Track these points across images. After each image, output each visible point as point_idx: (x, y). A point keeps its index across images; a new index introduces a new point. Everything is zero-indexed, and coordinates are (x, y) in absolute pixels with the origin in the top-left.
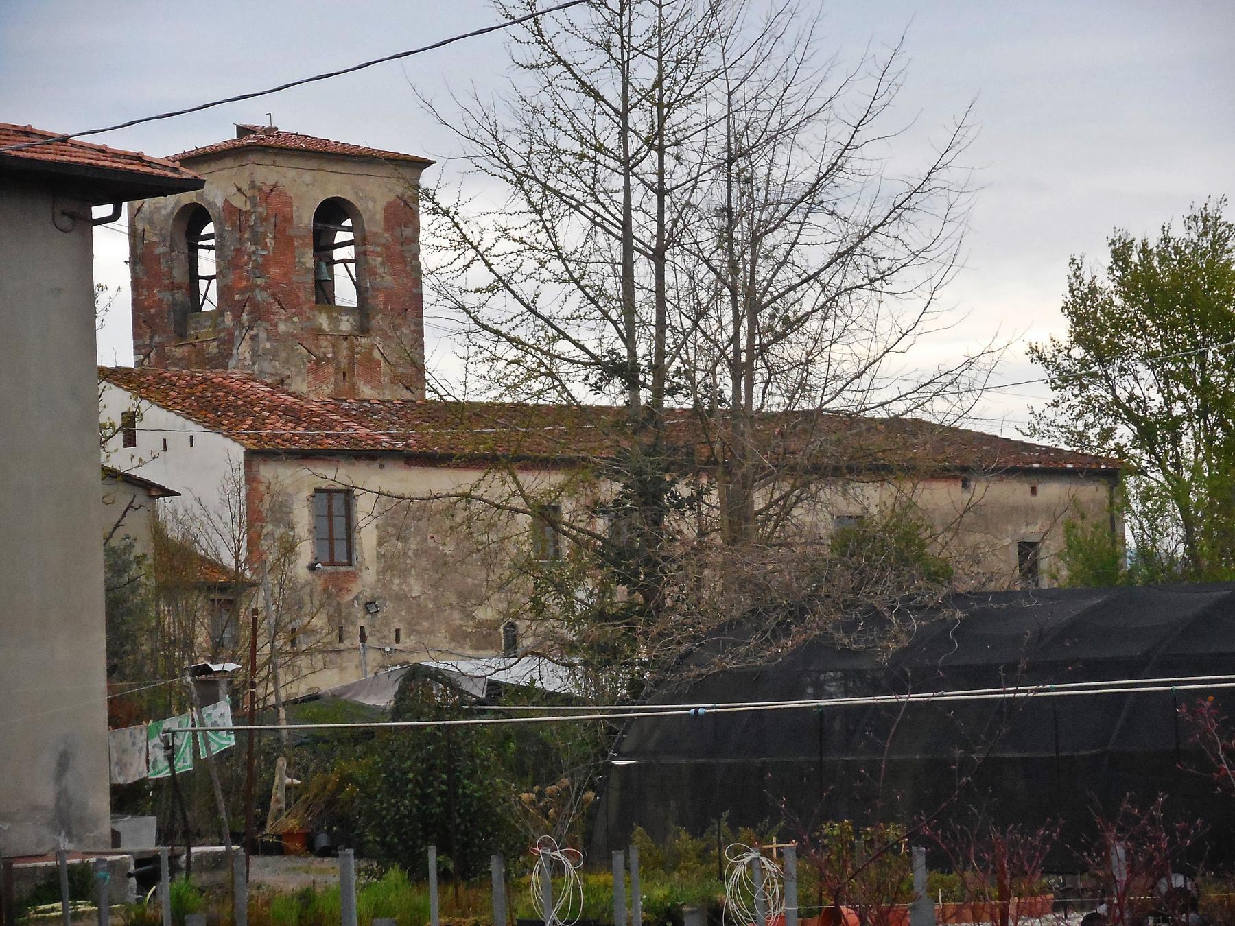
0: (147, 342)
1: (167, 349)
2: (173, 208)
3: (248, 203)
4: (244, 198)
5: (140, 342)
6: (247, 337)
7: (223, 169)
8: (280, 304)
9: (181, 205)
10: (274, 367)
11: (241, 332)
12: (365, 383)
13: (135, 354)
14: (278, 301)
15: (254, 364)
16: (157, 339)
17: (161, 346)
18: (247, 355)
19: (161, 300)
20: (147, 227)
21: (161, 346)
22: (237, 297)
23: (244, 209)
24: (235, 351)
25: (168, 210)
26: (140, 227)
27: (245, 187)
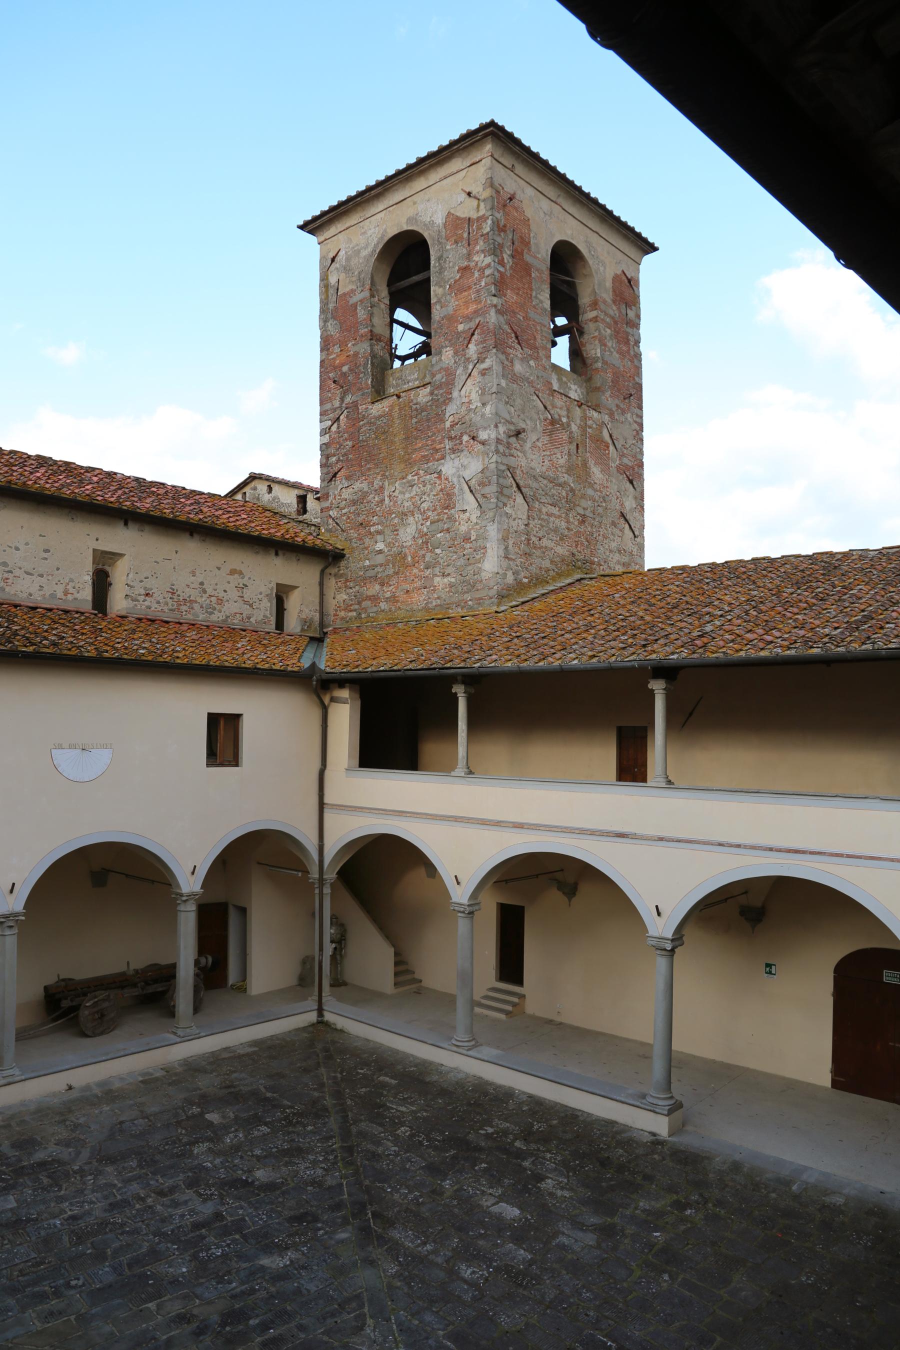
0: (337, 404)
1: (361, 408)
2: (376, 246)
3: (482, 205)
4: (475, 202)
5: (328, 406)
6: (475, 373)
7: (446, 178)
8: (517, 337)
9: (386, 239)
10: (509, 413)
11: (466, 368)
12: (596, 464)
13: (321, 422)
14: (516, 333)
15: (484, 404)
16: (348, 399)
17: (355, 405)
18: (474, 396)
19: (356, 354)
20: (342, 276)
21: (355, 405)
22: (461, 327)
23: (474, 215)
24: (455, 394)
25: (370, 249)
26: (333, 280)
27: (476, 189)
